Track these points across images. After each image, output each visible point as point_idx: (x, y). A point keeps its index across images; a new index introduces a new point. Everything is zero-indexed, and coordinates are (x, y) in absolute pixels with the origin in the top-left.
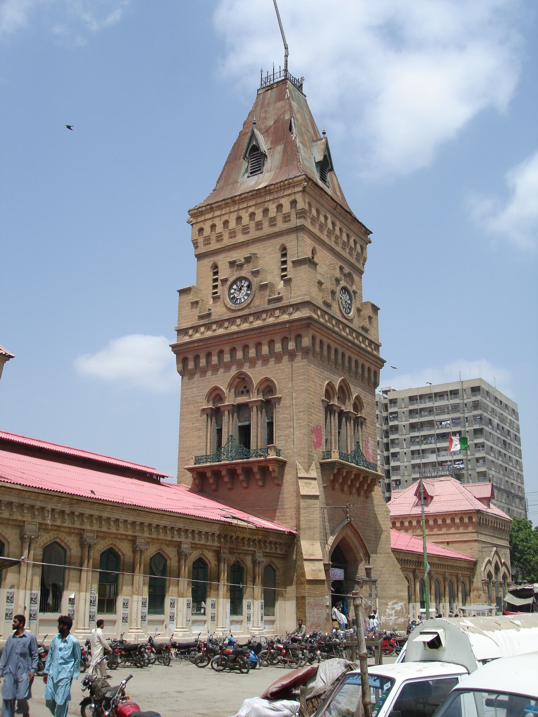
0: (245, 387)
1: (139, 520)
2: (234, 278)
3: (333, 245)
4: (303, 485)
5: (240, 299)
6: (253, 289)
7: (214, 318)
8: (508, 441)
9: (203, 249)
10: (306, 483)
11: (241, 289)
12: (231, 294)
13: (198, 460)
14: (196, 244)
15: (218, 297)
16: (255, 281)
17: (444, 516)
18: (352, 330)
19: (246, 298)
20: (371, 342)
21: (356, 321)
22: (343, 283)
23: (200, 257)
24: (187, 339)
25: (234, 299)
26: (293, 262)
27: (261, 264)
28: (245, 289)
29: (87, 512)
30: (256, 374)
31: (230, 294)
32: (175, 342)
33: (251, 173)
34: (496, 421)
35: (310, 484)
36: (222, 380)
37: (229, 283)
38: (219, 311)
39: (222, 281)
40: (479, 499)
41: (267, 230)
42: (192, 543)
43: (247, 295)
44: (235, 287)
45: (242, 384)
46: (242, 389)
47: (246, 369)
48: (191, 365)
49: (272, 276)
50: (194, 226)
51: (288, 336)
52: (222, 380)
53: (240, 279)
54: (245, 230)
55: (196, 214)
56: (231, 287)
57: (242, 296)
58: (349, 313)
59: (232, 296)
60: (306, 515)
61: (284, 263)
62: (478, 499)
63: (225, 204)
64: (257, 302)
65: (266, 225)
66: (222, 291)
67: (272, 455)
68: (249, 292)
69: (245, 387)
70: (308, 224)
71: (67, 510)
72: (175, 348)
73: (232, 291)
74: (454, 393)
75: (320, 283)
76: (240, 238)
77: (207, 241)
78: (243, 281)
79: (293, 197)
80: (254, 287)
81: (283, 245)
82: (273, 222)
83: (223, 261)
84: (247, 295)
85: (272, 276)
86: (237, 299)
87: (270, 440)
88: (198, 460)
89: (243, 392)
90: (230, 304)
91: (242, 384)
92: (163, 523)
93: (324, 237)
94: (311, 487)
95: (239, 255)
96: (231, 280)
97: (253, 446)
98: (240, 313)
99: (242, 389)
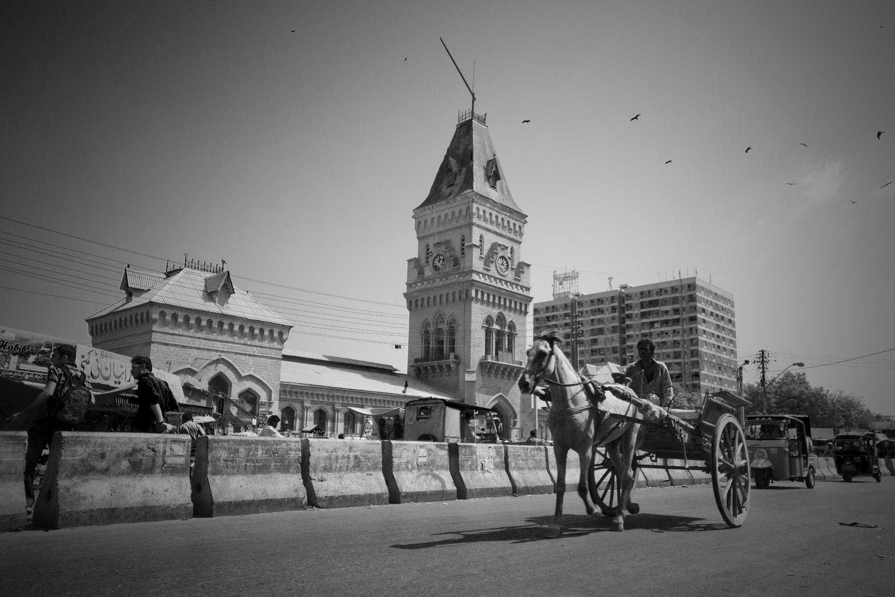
1: (364, 397)
3: (496, 230)
18: (506, 282)
20: (522, 287)
29: (336, 394)
32: (405, 291)
36: (429, 314)
41: (454, 224)
45: (440, 318)
52: (429, 314)
53: (439, 255)
71: (325, 393)
72: (405, 295)
74: (674, 289)
91: (440, 318)
92: (379, 398)
95: (437, 239)
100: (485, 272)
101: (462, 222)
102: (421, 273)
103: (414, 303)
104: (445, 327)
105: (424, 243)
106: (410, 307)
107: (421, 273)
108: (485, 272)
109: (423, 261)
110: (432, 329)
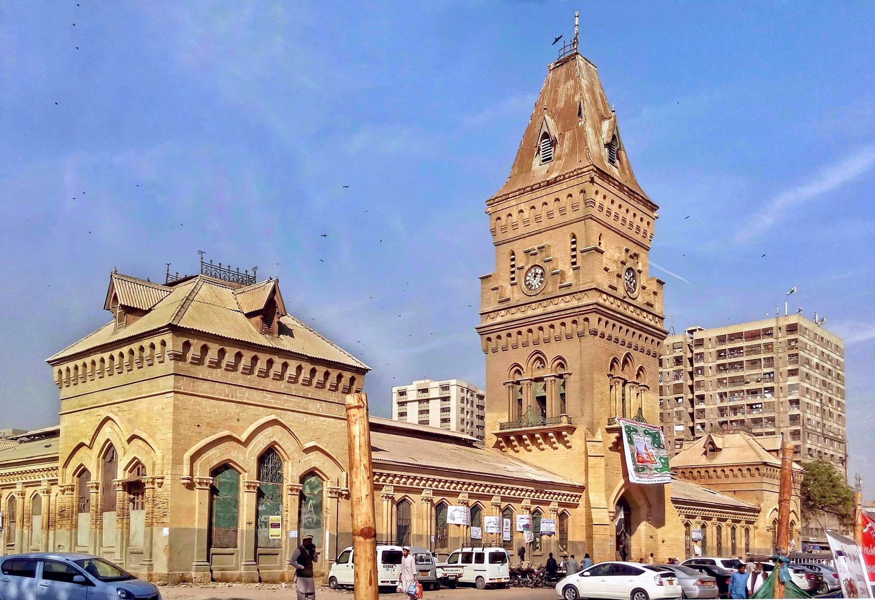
2: (530, 266)
7: (512, 303)
8: (828, 381)
9: (501, 237)
11: (535, 277)
13: (502, 427)
14: (493, 232)
15: (515, 284)
16: (548, 267)
17: (731, 467)
21: (639, 299)
22: (628, 265)
25: (529, 286)
26: (582, 252)
27: (554, 253)
30: (550, 352)
31: (526, 281)
34: (815, 360)
36: (521, 356)
37: (525, 271)
38: (516, 296)
39: (519, 269)
40: (769, 451)
43: (541, 282)
44: (530, 274)
47: (542, 348)
49: (564, 265)
54: (538, 219)
55: (492, 202)
56: (526, 275)
57: (535, 282)
58: (633, 292)
61: (574, 250)
62: (769, 451)
64: (550, 289)
65: (557, 214)
66: (519, 276)
67: (564, 423)
70: (594, 211)
73: (528, 278)
75: (606, 269)
76: (534, 227)
77: (504, 229)
80: (548, 275)
82: (562, 211)
83: (519, 247)
84: (541, 282)
85: (564, 265)
87: (563, 410)
88: (502, 427)
90: (526, 290)
95: (532, 244)
96: (527, 268)
97: (548, 415)
98: (534, 299)
100: (610, 291)
101: (571, 216)
104: (547, 373)
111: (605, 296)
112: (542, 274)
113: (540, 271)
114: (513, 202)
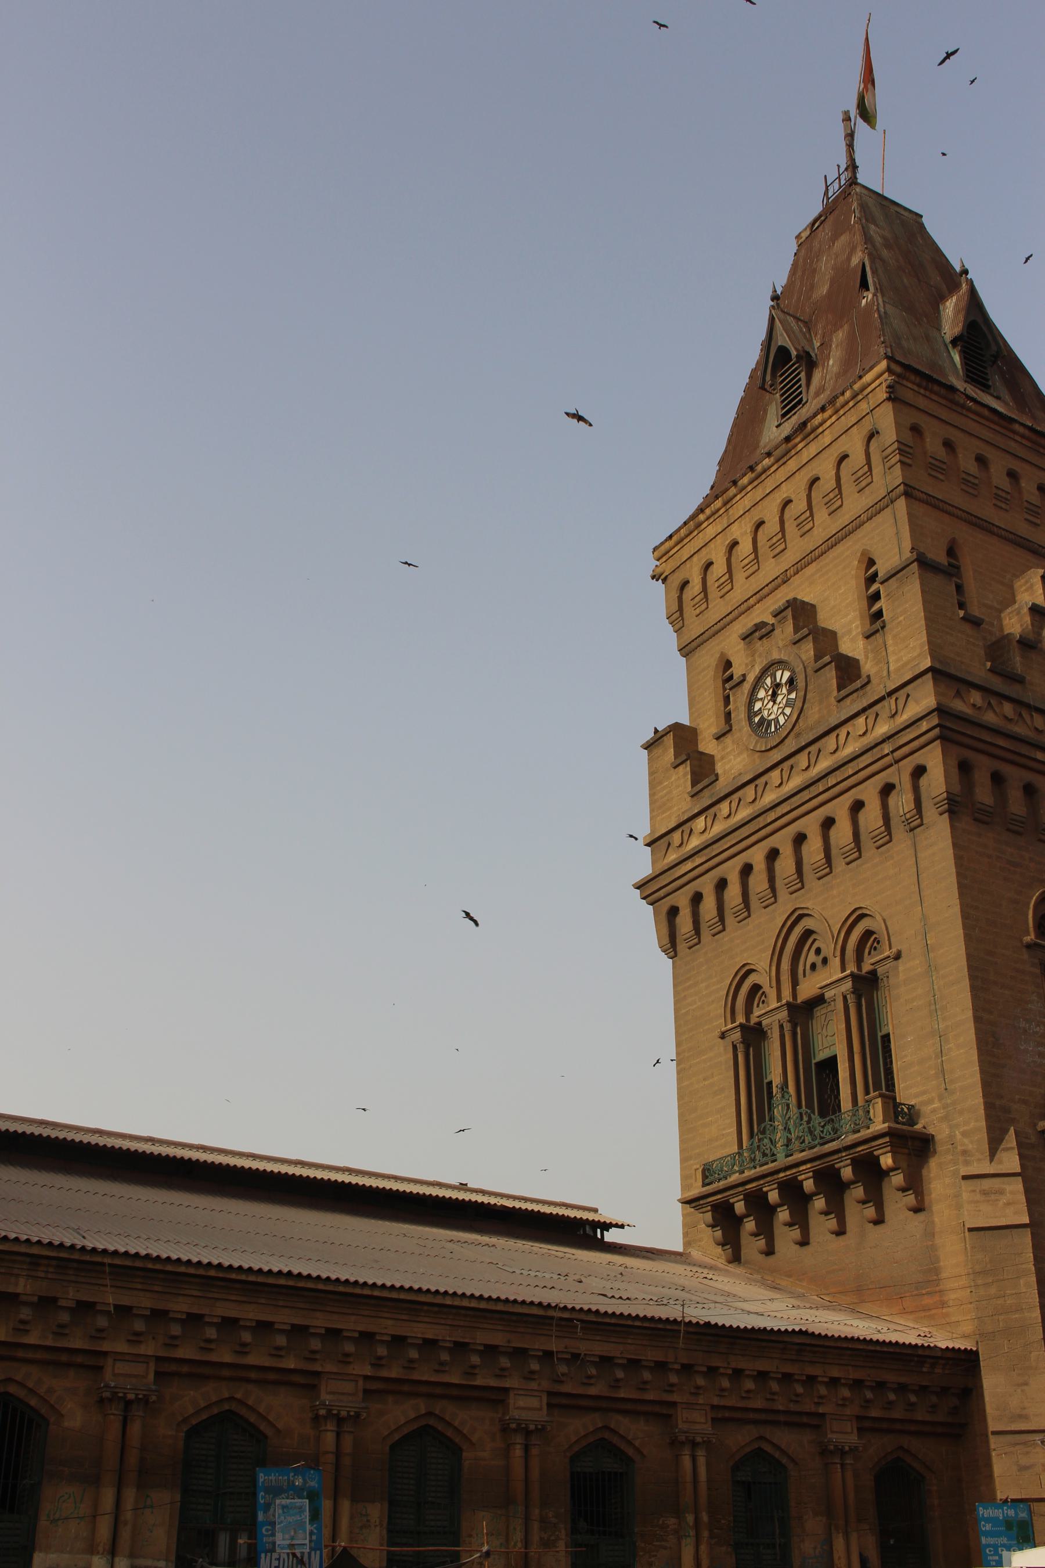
0: (818, 951)
2: (757, 669)
4: (978, 1197)
5: (777, 720)
6: (800, 682)
7: (723, 785)
10: (984, 1193)
11: (774, 695)
12: (756, 714)
19: (788, 711)
23: (687, 650)
24: (672, 857)
28: (784, 691)
31: (751, 714)
33: (783, 416)
35: (1001, 1192)
37: (747, 686)
42: (550, 1394)
44: (761, 694)
46: (812, 958)
48: (684, 923)
50: (669, 581)
51: (894, 780)
52: (752, 942)
57: (776, 710)
59: (757, 719)
60: (993, 1291)
63: (725, 504)
64: (813, 713)
68: (793, 696)
69: (818, 951)
73: (758, 706)
78: (779, 674)
79: (867, 426)
81: (864, 553)
86: (769, 725)
89: (813, 967)
90: (753, 741)
92: (420, 1330)
93: (986, 510)
94: (1001, 1203)
96: (751, 678)
98: (776, 756)
99: (812, 958)
100: (997, 683)
102: (702, 769)
103: (682, 905)
105: (708, 658)
106: (671, 945)
107: (702, 769)
108: (997, 683)
109: (708, 727)
110: (771, 1012)
111: (976, 697)
112: (791, 681)
113: (787, 675)
114: (711, 531)
